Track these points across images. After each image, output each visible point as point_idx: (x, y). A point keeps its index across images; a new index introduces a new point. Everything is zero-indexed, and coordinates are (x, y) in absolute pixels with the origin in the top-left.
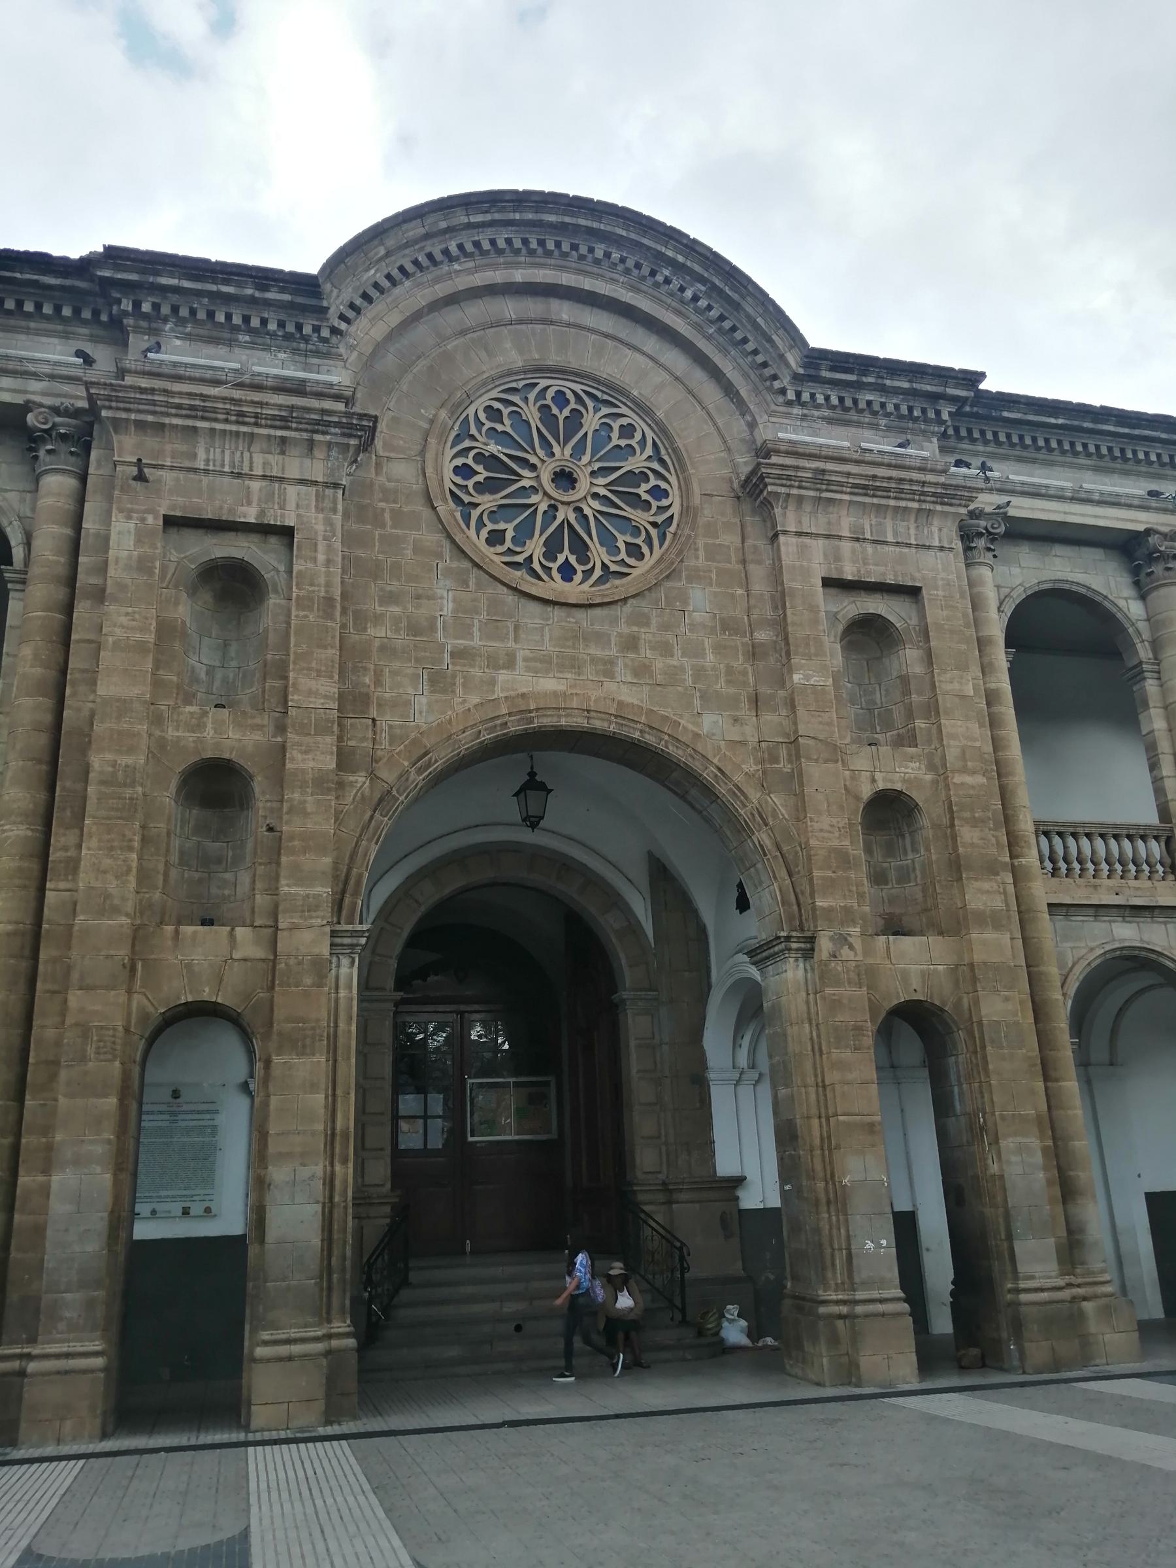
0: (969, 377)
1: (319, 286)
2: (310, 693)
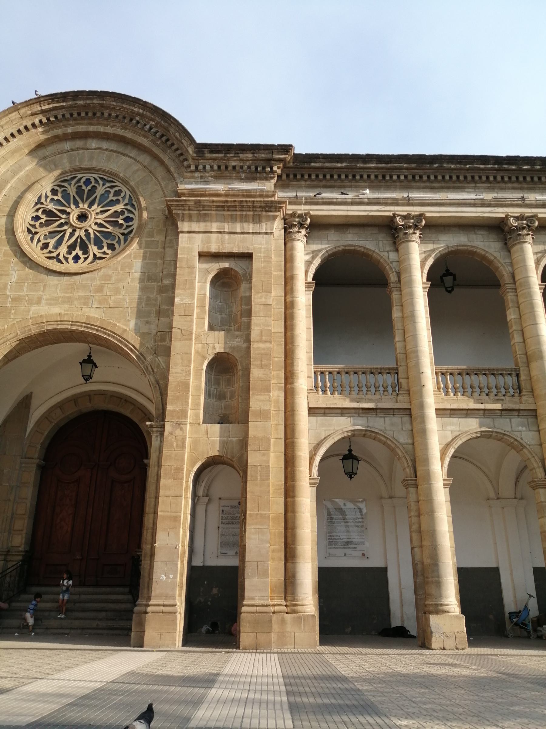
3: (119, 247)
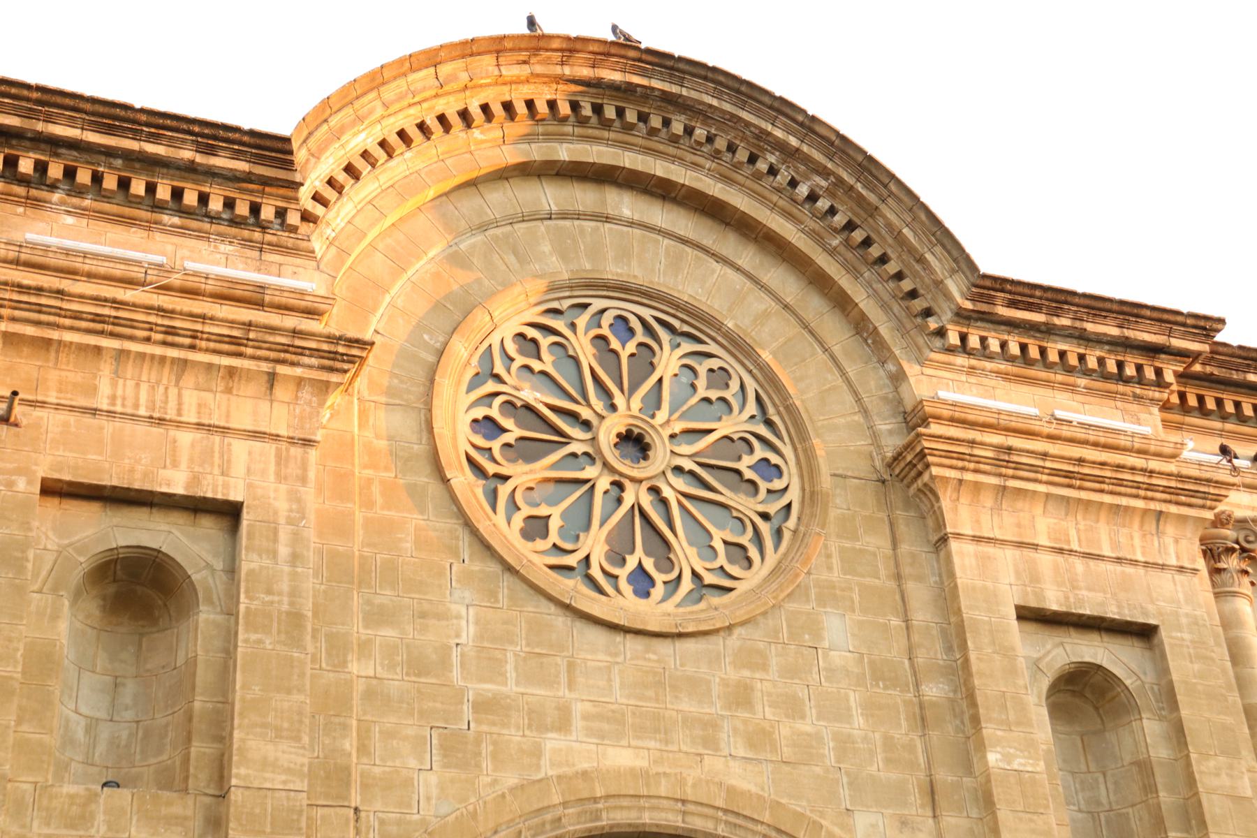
0: (1202, 323)
1: (291, 153)
2: (265, 764)
3: (763, 559)
